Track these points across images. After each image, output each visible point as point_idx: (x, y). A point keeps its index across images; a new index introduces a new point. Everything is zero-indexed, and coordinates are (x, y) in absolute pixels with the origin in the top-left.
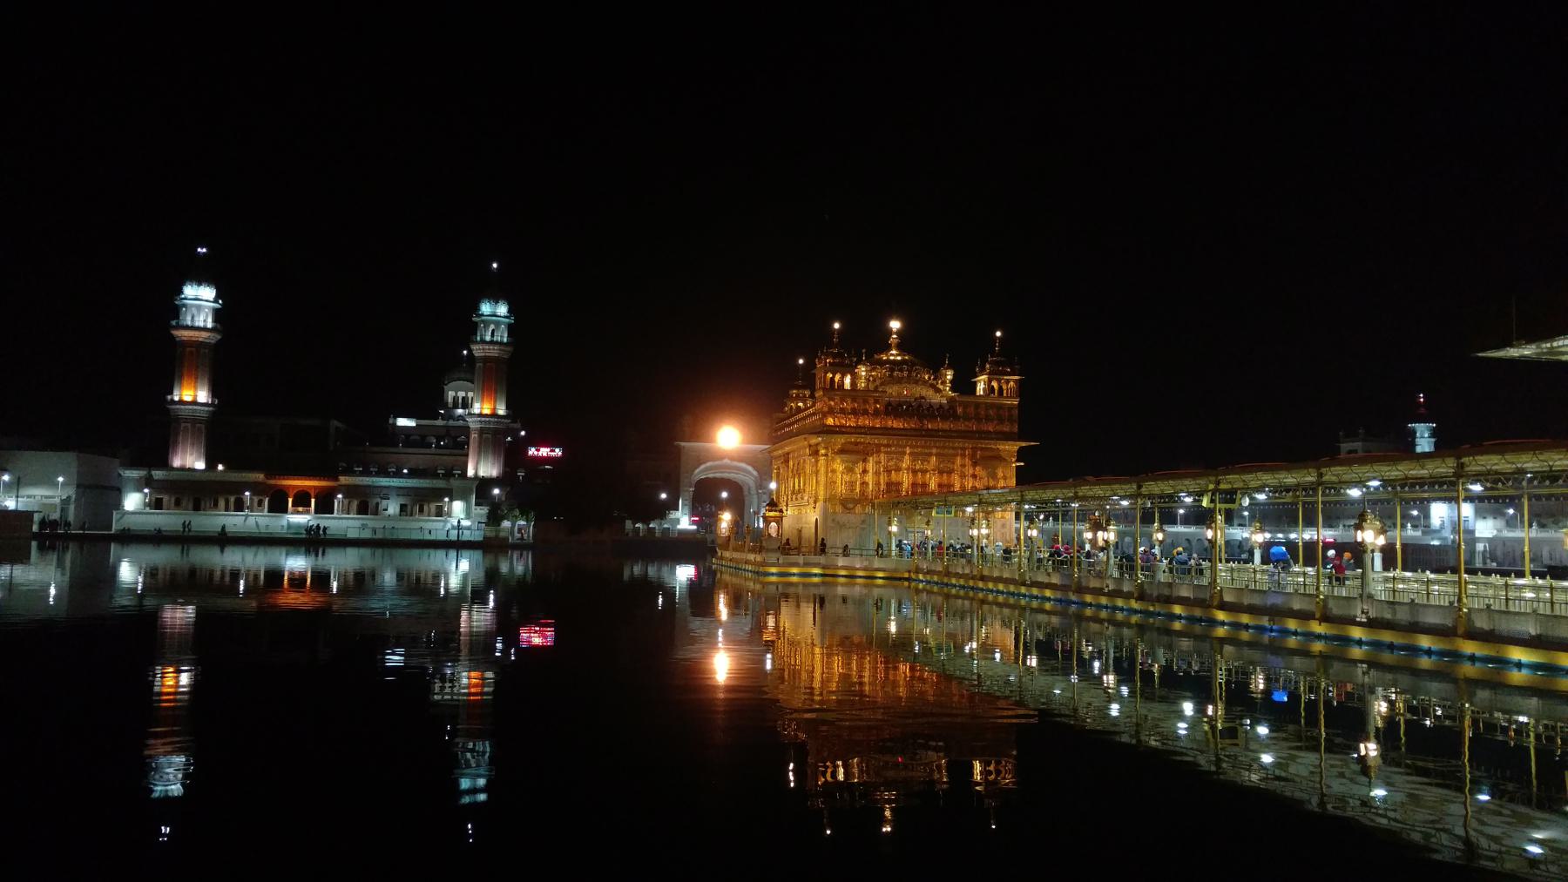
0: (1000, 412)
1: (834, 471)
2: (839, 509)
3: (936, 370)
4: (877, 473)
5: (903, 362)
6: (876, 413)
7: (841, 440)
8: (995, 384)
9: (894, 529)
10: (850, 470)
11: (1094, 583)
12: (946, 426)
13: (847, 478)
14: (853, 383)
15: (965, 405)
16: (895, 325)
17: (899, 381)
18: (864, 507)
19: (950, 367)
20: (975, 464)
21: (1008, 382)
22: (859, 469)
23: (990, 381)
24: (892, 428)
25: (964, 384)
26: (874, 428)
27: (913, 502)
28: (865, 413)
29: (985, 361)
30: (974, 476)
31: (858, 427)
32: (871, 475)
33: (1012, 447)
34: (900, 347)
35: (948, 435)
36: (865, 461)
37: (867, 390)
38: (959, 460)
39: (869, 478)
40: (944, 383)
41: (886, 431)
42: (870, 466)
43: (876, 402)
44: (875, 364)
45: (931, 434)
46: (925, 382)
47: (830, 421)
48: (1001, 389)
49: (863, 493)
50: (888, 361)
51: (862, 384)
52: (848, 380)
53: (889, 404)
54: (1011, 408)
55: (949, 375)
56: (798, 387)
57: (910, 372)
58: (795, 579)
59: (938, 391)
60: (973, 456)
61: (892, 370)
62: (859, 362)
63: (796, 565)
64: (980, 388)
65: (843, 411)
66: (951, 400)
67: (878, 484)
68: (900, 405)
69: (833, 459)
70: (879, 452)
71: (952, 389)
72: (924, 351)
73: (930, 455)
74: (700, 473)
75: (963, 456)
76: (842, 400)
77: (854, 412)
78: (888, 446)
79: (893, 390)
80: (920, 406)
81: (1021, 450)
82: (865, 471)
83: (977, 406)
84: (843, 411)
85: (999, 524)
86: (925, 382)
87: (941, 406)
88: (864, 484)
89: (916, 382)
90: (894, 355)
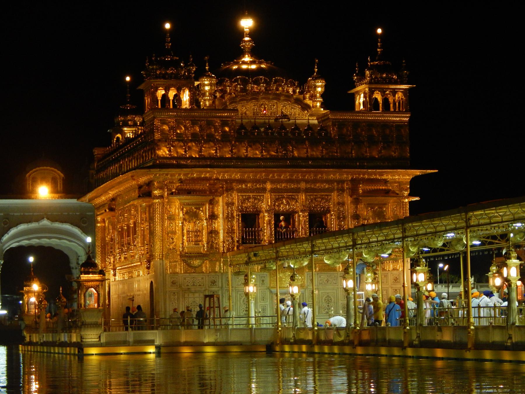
0: (385, 132)
1: (171, 218)
2: (180, 268)
3: (302, 80)
4: (229, 218)
5: (259, 71)
6: (226, 138)
7: (178, 175)
8: (378, 96)
9: (251, 289)
10: (192, 215)
11: (497, 337)
12: (316, 153)
13: (189, 226)
14: (194, 100)
15: (341, 124)
16: (247, 23)
17: (255, 96)
18: (213, 263)
19: (320, 76)
20: (356, 202)
21: (394, 92)
22: (204, 213)
23: (372, 92)
24: (247, 158)
25: (338, 98)
26: (222, 158)
28: (210, 139)
29: (363, 67)
30: (356, 217)
31: (202, 158)
33: (405, 176)
34: (253, 52)
35: (319, 164)
36: (212, 203)
37: (212, 108)
38: (334, 196)
39: (220, 225)
40: (313, 97)
42: (220, 209)
43: (225, 123)
44: (223, 77)
45: (296, 164)
46: (288, 97)
47: (163, 152)
48: (386, 101)
49: (211, 245)
50: (239, 71)
51: (206, 102)
52: (186, 97)
53: (242, 126)
54: (399, 126)
55: (320, 87)
56: (125, 113)
57: (268, 84)
58: (122, 357)
59: (306, 107)
60: (353, 191)
61: (245, 83)
62: (200, 74)
63: (125, 343)
64: (360, 100)
65: (180, 138)
66: (322, 119)
67: (230, 232)
68: (255, 127)
69: (170, 203)
70: (229, 190)
71: (323, 105)
72: (288, 57)
73: (298, 191)
75: (341, 190)
76: (178, 123)
77: (195, 138)
78: (241, 181)
79: (247, 110)
80: (283, 127)
81: (415, 181)
82: (213, 217)
83: (356, 124)
84: (180, 138)
85: (391, 278)
86: (288, 97)
87: (310, 127)
88: (213, 233)
89: (277, 97)
90: (247, 63)
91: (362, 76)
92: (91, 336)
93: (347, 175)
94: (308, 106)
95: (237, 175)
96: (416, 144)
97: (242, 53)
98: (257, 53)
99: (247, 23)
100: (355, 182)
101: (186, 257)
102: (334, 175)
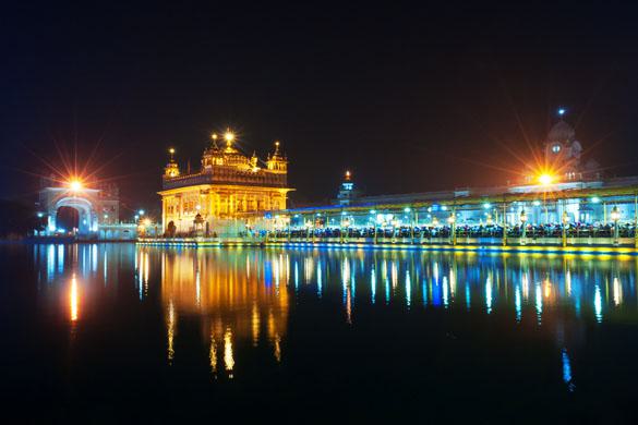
3: (249, 157)
10: (222, 201)
15: (267, 173)
25: (262, 164)
27: (252, 213)
32: (231, 203)
33: (284, 191)
34: (231, 147)
39: (231, 204)
41: (238, 184)
55: (256, 160)
65: (219, 175)
72: (244, 150)
74: (59, 204)
77: (224, 175)
83: (271, 174)
90: (229, 150)
91: (271, 158)
92: (199, 239)
93: (269, 189)
94: (251, 166)
95: (237, 187)
96: (289, 181)
97: (226, 147)
98: (233, 146)
99: (229, 137)
100: (271, 192)
101: (221, 214)
102: (265, 189)
